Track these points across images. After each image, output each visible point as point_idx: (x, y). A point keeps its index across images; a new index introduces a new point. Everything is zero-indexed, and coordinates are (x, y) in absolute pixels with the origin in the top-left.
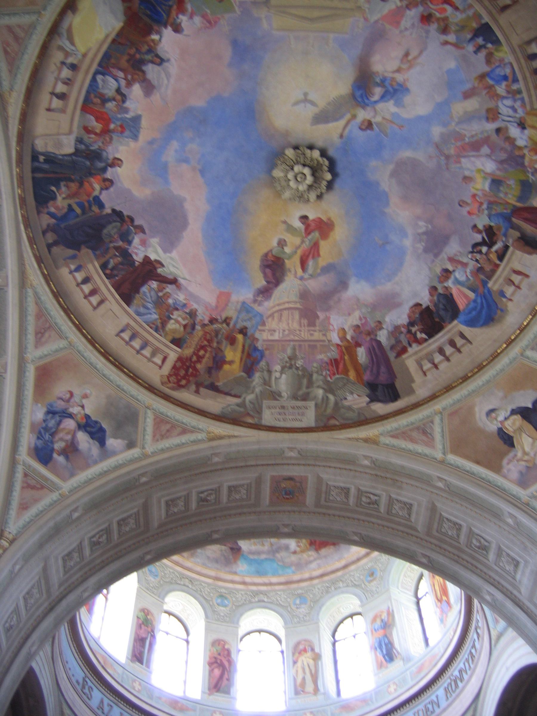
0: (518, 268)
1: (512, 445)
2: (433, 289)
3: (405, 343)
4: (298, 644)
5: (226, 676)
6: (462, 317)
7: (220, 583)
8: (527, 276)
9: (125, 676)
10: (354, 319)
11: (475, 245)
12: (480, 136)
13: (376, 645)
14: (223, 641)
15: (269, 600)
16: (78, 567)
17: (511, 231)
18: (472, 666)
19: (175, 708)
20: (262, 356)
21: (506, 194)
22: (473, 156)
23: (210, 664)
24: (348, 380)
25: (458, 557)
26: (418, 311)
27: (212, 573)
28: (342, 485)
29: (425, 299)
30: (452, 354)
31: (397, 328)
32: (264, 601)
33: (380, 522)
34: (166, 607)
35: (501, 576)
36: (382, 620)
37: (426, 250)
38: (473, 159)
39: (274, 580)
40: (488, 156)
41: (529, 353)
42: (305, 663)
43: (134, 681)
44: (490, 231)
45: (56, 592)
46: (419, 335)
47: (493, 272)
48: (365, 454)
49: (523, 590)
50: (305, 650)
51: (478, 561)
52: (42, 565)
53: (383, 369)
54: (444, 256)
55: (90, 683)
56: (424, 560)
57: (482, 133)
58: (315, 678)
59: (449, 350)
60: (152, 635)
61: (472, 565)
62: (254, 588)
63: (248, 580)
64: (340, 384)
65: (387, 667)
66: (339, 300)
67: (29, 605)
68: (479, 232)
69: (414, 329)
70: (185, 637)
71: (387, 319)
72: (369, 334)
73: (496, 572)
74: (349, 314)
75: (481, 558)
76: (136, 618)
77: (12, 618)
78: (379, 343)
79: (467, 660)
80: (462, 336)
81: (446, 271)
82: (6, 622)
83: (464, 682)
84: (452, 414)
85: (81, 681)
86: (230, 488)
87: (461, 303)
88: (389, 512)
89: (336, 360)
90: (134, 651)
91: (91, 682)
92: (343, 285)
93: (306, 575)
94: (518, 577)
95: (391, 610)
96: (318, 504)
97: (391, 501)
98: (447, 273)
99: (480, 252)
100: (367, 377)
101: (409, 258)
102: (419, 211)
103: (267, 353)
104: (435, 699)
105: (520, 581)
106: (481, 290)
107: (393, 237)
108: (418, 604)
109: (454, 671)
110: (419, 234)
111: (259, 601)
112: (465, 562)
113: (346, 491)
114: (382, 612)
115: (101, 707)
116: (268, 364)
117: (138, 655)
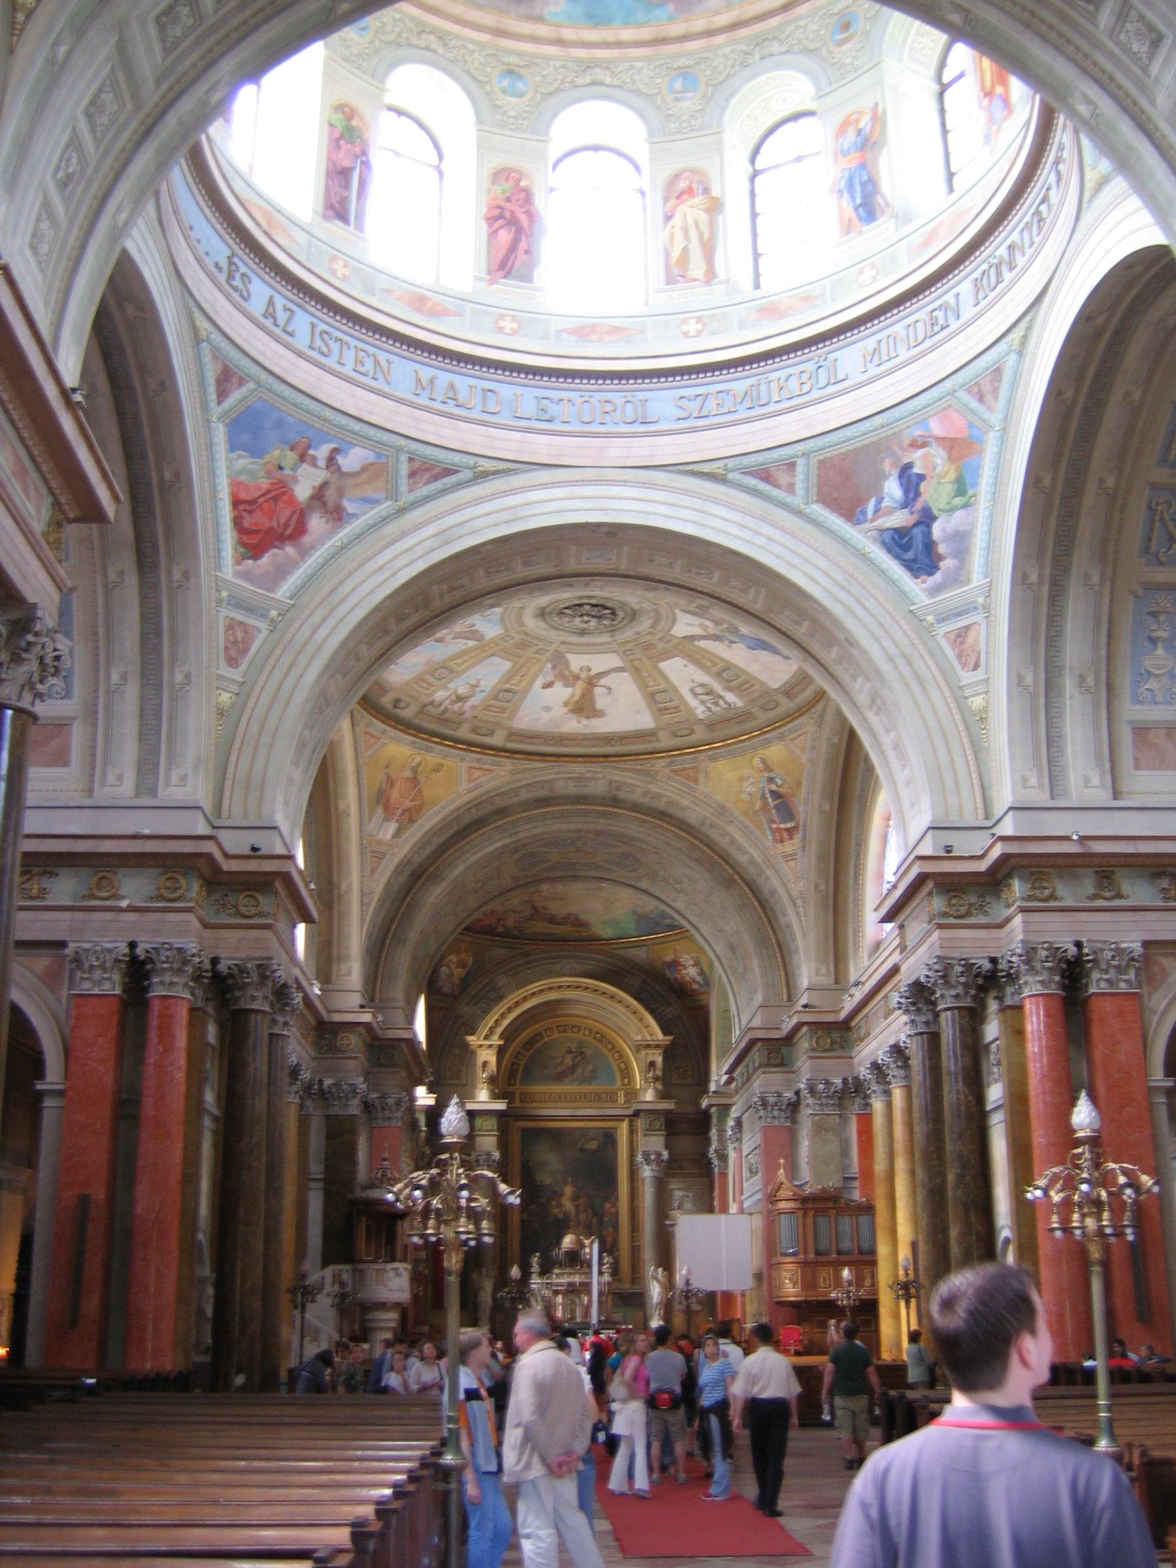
4: (677, 177)
5: (523, 245)
9: (313, 250)
13: (843, 184)
14: (515, 171)
15: (615, 82)
16: (193, 37)
18: (1037, 240)
19: (419, 310)
23: (491, 220)
25: (1033, 14)
27: (489, 20)
32: (602, 84)
34: (389, 99)
35: (1118, 63)
36: (859, 132)
39: (627, 35)
42: (690, 220)
43: (334, 259)
45: (152, 97)
49: (1160, 99)
50: (690, 192)
51: (1073, 25)
52: (113, 41)
55: (243, 269)
56: (955, 18)
58: (709, 249)
60: (362, 162)
61: (1060, 35)
62: (582, 53)
63: (568, 34)
65: (860, 233)
67: (99, 129)
70: (433, 158)
73: (1110, 55)
75: (1082, 21)
76: (326, 128)
77: (68, 160)
79: (1028, 226)
82: (58, 168)
83: (1015, 271)
85: (224, 263)
90: (327, 196)
91: (246, 264)
93: (699, 25)
94: (1155, 68)
95: (880, 112)
104: (952, 302)
105: (1157, 79)
108: (941, 95)
109: (997, 248)
111: (593, 83)
112: (1044, 27)
114: (861, 113)
115: (270, 313)
117: (337, 206)
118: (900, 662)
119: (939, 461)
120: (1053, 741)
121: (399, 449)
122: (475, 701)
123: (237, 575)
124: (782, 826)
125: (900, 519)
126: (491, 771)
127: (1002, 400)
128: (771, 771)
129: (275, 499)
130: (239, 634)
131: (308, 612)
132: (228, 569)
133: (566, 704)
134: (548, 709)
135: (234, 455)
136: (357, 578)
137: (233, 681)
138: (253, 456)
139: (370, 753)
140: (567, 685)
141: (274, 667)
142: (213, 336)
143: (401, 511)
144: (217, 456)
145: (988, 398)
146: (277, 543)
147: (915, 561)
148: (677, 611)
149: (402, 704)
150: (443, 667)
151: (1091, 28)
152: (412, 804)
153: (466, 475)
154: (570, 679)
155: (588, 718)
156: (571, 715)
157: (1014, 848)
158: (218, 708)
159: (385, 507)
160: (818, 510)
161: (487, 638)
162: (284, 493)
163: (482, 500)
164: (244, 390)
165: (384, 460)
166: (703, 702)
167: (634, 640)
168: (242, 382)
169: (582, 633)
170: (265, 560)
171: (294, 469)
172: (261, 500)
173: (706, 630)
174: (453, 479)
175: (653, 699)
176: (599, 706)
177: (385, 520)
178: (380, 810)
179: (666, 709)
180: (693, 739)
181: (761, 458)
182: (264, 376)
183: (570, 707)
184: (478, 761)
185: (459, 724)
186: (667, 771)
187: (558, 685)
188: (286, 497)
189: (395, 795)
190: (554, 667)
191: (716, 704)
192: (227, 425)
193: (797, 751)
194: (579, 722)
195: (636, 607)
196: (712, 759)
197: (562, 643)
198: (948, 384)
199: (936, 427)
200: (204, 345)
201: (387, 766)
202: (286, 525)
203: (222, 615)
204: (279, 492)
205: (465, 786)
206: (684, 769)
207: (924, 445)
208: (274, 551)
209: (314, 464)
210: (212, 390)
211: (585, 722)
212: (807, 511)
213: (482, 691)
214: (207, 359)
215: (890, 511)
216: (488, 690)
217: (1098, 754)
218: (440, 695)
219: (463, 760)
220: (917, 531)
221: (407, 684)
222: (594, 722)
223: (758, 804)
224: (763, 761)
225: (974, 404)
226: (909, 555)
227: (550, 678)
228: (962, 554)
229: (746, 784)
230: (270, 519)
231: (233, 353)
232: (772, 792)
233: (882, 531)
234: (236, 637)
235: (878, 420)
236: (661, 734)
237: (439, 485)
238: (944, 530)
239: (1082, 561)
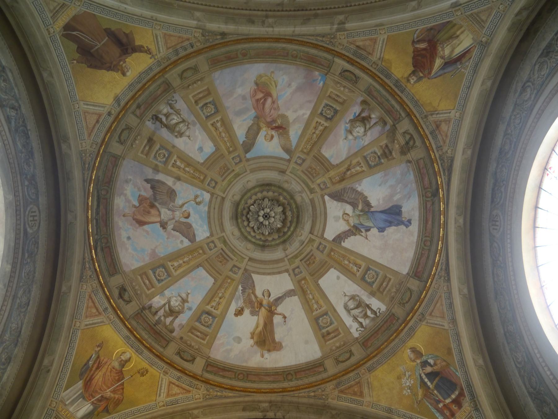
122: (183, 319)
124: (448, 401)
126: (189, 391)
128: (422, 355)
133: (252, 335)
134: (238, 340)
139: (89, 321)
140: (253, 313)
148: (327, 198)
149: (126, 297)
150: (163, 266)
152: (112, 395)
155: (269, 351)
156: (256, 347)
161: (198, 239)
166: (355, 318)
167: (300, 253)
176: (277, 338)
178: (80, 384)
179: (328, 333)
183: (255, 338)
184: (178, 379)
185: (168, 342)
186: (336, 392)
187: (247, 312)
189: (99, 377)
190: (243, 291)
191: (366, 316)
194: (262, 356)
196: (370, 370)
197: (251, 259)
201: (100, 346)
205: (163, 398)
206: (350, 387)
211: (266, 355)
213: (190, 309)
216: (194, 309)
218: (158, 301)
219: (166, 373)
222: (274, 355)
223: (420, 392)
224: (414, 350)
227: (241, 303)
229: (403, 381)
232: (428, 375)
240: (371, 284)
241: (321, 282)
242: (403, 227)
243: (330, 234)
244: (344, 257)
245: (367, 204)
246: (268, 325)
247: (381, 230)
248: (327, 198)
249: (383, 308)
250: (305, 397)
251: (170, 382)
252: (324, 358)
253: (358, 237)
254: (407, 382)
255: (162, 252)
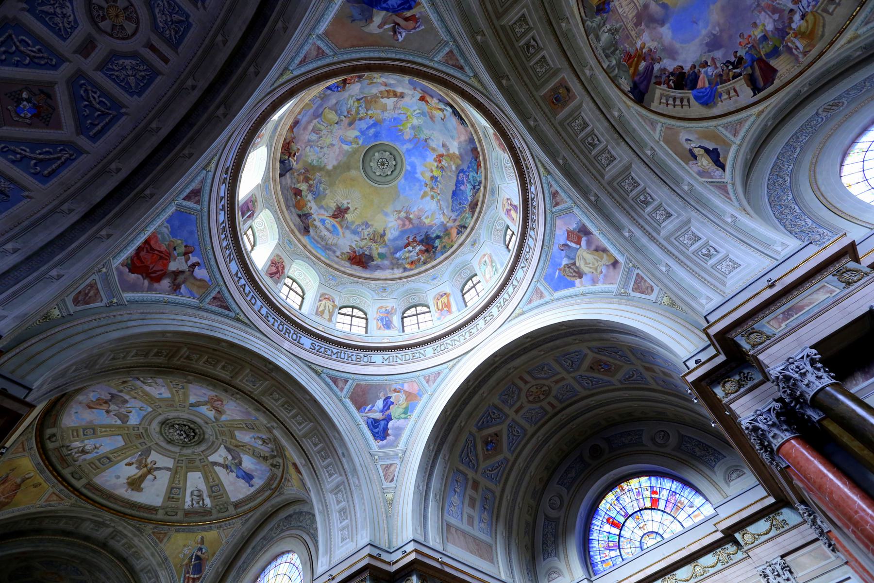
0: (737, 89)
1: (696, 159)
2: (694, 66)
3: (663, 80)
6: (695, 91)
7: (292, 235)
8: (738, 96)
10: (652, 45)
11: (728, 62)
12: (782, 6)
17: (749, 68)
20: (608, 12)
21: (763, 47)
22: (769, 15)
23: (272, 262)
24: (628, 71)
26: (680, 70)
28: (587, 120)
29: (687, 68)
30: (678, 105)
31: (665, 69)
33: (585, 161)
37: (707, 44)
38: (767, 16)
40: (775, 21)
41: (720, 128)
44: (740, 59)
46: (671, 83)
47: (725, 81)
48: (621, 108)
51: (635, 210)
53: (645, 83)
54: (712, 54)
56: (593, 199)
57: (785, 5)
59: (678, 102)
64: (624, 69)
66: (655, 28)
68: (736, 57)
69: (671, 78)
71: (665, 61)
72: (652, 59)
74: (653, 40)
78: (653, 68)
80: (688, 101)
81: (706, 63)
84: (667, 128)
86: (544, 57)
87: (700, 85)
88: (595, 157)
89: (631, 55)
92: (662, 23)
96: (561, 123)
97: (605, 149)
98: (705, 64)
99: (728, 67)
100: (637, 78)
101: (697, 41)
102: (722, 21)
103: (611, 13)
106: (713, 86)
107: (701, 24)
110: (711, 33)
113: (585, 125)
116: (607, 18)
118: (364, 468)
119: (401, 399)
120: (425, 517)
121: (218, 285)
123: (117, 269)
124: (192, 576)
125: (378, 416)
126: (62, 500)
127: (436, 384)
129: (161, 258)
130: (92, 293)
131: (132, 312)
132: (117, 262)
133: (129, 478)
134: (118, 477)
135: (166, 224)
136: (164, 316)
137: (67, 309)
138: (171, 233)
139: (13, 456)
141: (95, 320)
142: (210, 173)
143: (199, 308)
144: (161, 217)
145: (431, 382)
146: (144, 275)
147: (377, 433)
148: (222, 446)
151: (641, 212)
153: (233, 315)
154: (141, 464)
156: (126, 485)
157: (420, 558)
158: (47, 313)
159: (194, 302)
160: (348, 402)
162: (166, 259)
163: (233, 327)
164: (195, 206)
165: (210, 284)
166: (192, 500)
167: (189, 456)
168: (198, 202)
169: (170, 442)
170: (133, 276)
171: (179, 255)
172: (156, 252)
173: (225, 461)
174: (227, 312)
175: (171, 490)
177: (190, 306)
179: (173, 498)
180: (174, 518)
181: (337, 373)
182: (206, 209)
184: (60, 491)
186: (150, 532)
187: (135, 466)
188: (165, 261)
190: (140, 455)
191: (198, 503)
192: (176, 210)
193: (223, 536)
195: (207, 436)
196: (177, 531)
197: (156, 444)
198: (418, 373)
199: (406, 387)
200: (205, 172)
201: (13, 470)
202: (155, 272)
203: (93, 277)
204: (165, 257)
205: (42, 502)
207: (398, 392)
208: (140, 276)
209: (186, 262)
210: (188, 191)
211: (129, 491)
212: (344, 400)
214: (199, 178)
215: (375, 412)
217: (438, 528)
220: (383, 423)
221: (68, 428)
223: (186, 561)
224: (202, 538)
225: (424, 383)
226: (376, 430)
227: (134, 460)
228: (398, 436)
230: (151, 263)
231: (207, 189)
232: (197, 556)
233: (369, 418)
234: (89, 292)
235: (386, 377)
236: (161, 512)
237: (220, 310)
238: (393, 425)
239: (445, 448)
240: (213, 492)
241: (189, 474)
242: (248, 485)
243: (211, 459)
244: (210, 472)
245: (240, 464)
246: (142, 478)
247: (238, 477)
248: (222, 446)
249: (209, 505)
250: (131, 525)
251: (54, 493)
252: (160, 508)
253: (224, 470)
254: (186, 551)
255: (97, 422)
